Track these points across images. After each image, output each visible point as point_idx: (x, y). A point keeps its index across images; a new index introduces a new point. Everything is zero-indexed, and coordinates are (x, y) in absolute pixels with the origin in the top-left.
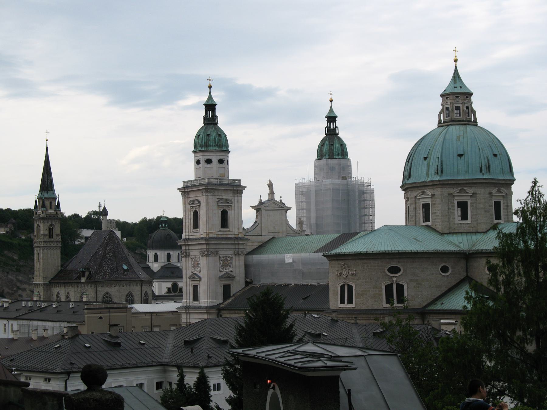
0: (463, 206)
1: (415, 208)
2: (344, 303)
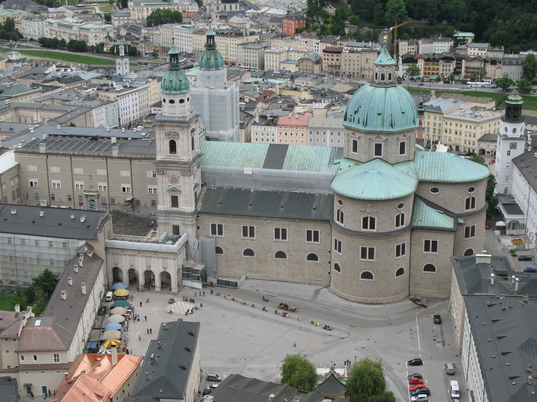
0: (402, 145)
1: (369, 146)
2: (367, 228)
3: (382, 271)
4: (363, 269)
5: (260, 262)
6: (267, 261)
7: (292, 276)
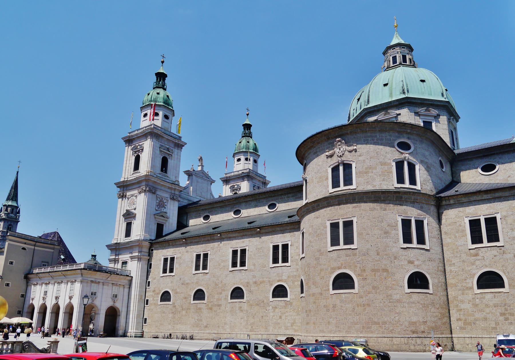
3: (373, 270)
4: (334, 269)
5: (211, 309)
6: (219, 305)
7: (251, 331)
